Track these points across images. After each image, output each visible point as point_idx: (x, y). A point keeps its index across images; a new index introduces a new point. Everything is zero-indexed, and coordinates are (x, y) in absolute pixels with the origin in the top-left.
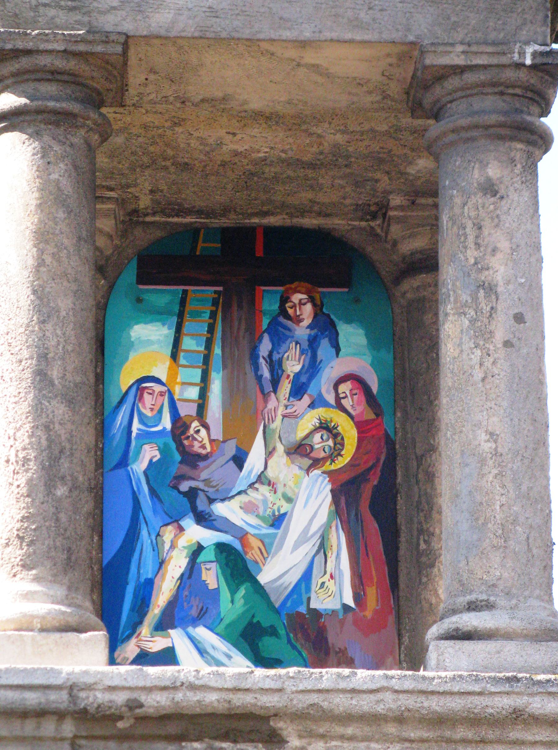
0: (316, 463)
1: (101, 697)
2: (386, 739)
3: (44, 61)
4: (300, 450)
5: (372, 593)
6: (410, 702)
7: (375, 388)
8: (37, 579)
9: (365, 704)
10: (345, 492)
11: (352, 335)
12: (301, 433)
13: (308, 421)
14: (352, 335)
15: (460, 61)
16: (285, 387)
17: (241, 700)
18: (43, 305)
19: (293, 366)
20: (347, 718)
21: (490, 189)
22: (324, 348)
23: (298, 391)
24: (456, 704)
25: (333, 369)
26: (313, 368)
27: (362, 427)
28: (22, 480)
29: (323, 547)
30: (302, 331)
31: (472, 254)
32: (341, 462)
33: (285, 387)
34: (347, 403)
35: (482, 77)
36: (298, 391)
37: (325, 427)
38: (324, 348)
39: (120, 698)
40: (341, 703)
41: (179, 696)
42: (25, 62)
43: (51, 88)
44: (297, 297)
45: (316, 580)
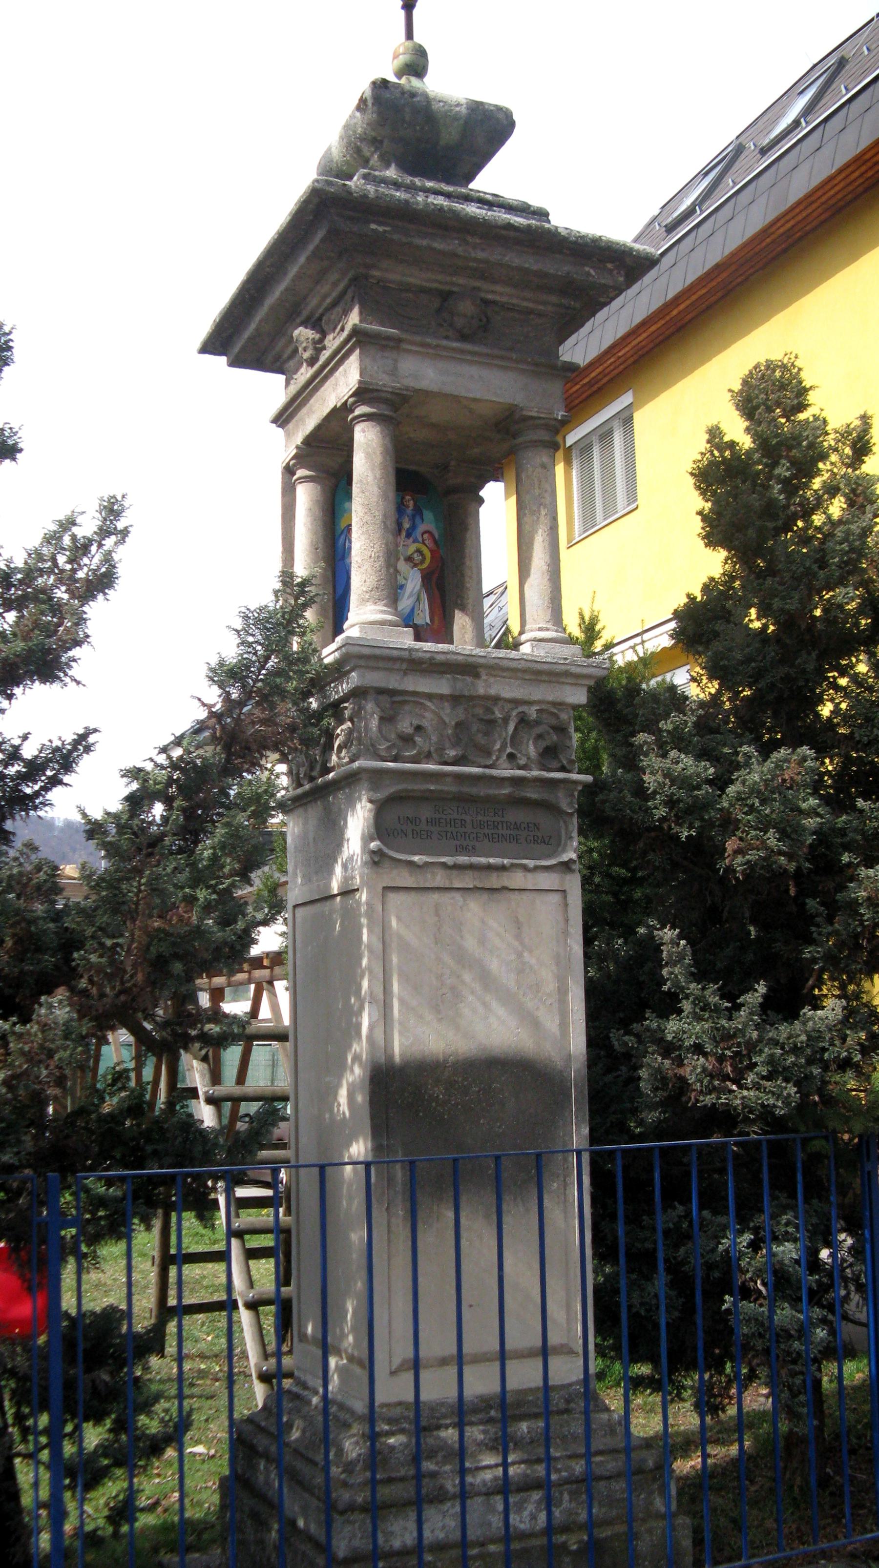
0: (415, 565)
1: (420, 654)
2: (517, 678)
3: (383, 395)
4: (409, 559)
5: (436, 619)
6: (529, 665)
7: (437, 537)
8: (385, 605)
9: (514, 665)
10: (426, 578)
11: (428, 515)
12: (409, 553)
13: (412, 548)
14: (428, 515)
15: (535, 414)
16: (404, 534)
17: (471, 660)
18: (385, 496)
19: (406, 525)
20: (508, 669)
21: (544, 466)
22: (418, 520)
23: (408, 535)
24: (545, 667)
25: (421, 528)
26: (414, 527)
27: (431, 551)
28: (377, 565)
29: (418, 599)
30: (409, 511)
31: (537, 492)
32: (425, 566)
33: (404, 534)
34: (427, 542)
35: (542, 422)
36: (408, 535)
37: (418, 551)
38: (418, 520)
39: (428, 655)
40: (505, 663)
41: (449, 657)
42: (375, 394)
43: (384, 406)
44: (408, 497)
45: (416, 612)
